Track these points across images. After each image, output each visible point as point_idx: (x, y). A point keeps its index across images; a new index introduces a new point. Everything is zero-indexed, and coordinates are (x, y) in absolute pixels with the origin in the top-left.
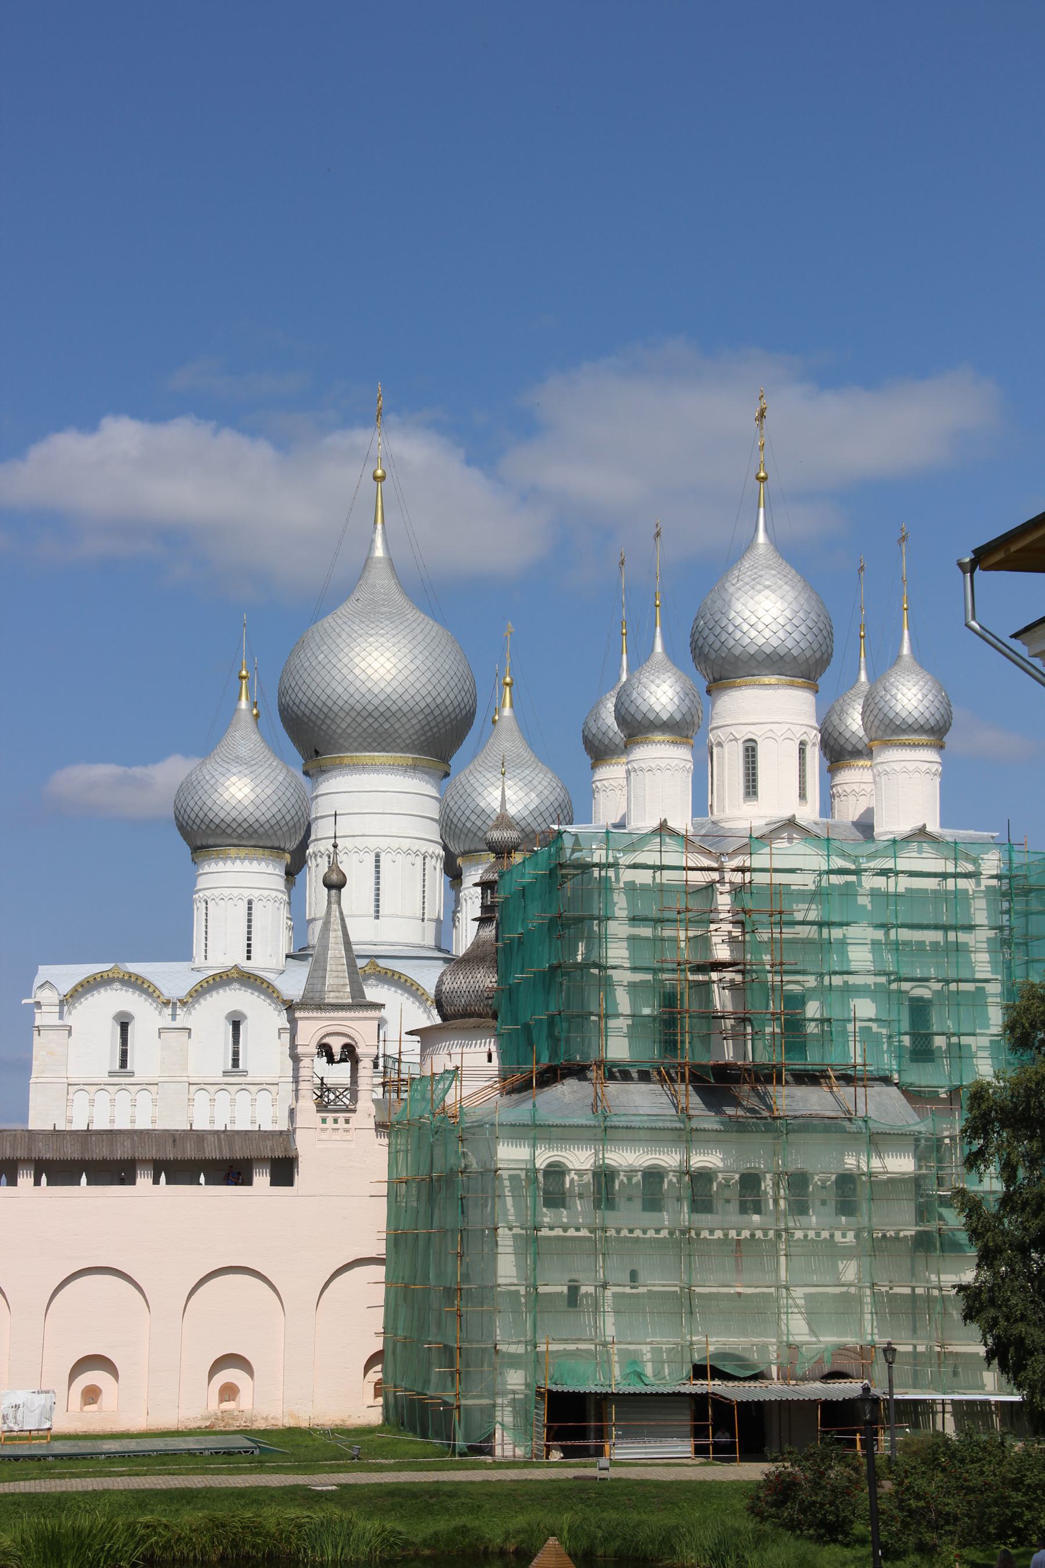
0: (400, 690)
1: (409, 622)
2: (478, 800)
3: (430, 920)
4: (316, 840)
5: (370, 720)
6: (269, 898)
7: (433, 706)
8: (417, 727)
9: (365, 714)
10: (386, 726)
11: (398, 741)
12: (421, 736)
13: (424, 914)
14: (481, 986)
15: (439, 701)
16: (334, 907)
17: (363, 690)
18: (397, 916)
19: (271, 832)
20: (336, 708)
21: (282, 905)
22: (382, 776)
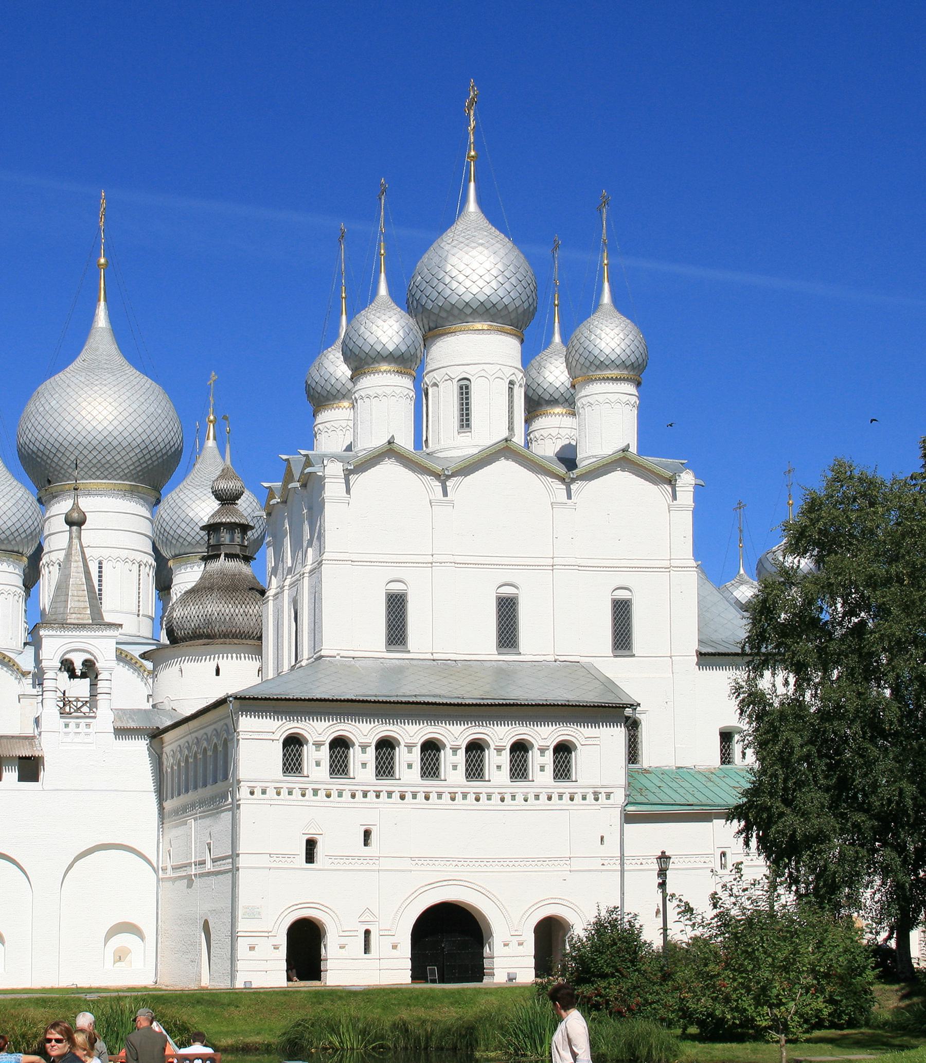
0: (121, 428)
1: (128, 375)
2: (188, 511)
3: (144, 616)
4: (50, 535)
5: (95, 453)
6: (10, 592)
7: (147, 442)
8: (134, 459)
9: (90, 448)
10: (108, 458)
11: (118, 470)
12: (138, 466)
13: (139, 611)
14: (210, 611)
15: (152, 438)
16: (75, 541)
17: (89, 428)
18: (117, 612)
19: (11, 538)
20: (66, 444)
21: (21, 598)
22: (105, 499)
